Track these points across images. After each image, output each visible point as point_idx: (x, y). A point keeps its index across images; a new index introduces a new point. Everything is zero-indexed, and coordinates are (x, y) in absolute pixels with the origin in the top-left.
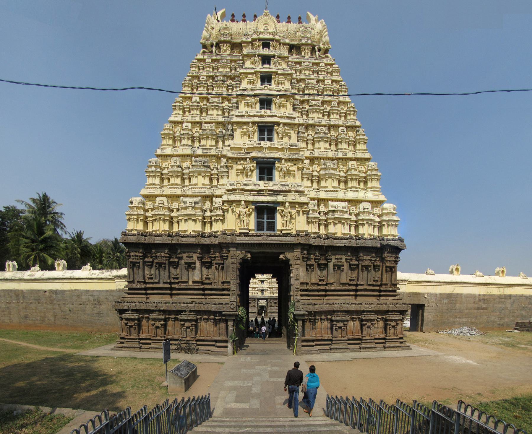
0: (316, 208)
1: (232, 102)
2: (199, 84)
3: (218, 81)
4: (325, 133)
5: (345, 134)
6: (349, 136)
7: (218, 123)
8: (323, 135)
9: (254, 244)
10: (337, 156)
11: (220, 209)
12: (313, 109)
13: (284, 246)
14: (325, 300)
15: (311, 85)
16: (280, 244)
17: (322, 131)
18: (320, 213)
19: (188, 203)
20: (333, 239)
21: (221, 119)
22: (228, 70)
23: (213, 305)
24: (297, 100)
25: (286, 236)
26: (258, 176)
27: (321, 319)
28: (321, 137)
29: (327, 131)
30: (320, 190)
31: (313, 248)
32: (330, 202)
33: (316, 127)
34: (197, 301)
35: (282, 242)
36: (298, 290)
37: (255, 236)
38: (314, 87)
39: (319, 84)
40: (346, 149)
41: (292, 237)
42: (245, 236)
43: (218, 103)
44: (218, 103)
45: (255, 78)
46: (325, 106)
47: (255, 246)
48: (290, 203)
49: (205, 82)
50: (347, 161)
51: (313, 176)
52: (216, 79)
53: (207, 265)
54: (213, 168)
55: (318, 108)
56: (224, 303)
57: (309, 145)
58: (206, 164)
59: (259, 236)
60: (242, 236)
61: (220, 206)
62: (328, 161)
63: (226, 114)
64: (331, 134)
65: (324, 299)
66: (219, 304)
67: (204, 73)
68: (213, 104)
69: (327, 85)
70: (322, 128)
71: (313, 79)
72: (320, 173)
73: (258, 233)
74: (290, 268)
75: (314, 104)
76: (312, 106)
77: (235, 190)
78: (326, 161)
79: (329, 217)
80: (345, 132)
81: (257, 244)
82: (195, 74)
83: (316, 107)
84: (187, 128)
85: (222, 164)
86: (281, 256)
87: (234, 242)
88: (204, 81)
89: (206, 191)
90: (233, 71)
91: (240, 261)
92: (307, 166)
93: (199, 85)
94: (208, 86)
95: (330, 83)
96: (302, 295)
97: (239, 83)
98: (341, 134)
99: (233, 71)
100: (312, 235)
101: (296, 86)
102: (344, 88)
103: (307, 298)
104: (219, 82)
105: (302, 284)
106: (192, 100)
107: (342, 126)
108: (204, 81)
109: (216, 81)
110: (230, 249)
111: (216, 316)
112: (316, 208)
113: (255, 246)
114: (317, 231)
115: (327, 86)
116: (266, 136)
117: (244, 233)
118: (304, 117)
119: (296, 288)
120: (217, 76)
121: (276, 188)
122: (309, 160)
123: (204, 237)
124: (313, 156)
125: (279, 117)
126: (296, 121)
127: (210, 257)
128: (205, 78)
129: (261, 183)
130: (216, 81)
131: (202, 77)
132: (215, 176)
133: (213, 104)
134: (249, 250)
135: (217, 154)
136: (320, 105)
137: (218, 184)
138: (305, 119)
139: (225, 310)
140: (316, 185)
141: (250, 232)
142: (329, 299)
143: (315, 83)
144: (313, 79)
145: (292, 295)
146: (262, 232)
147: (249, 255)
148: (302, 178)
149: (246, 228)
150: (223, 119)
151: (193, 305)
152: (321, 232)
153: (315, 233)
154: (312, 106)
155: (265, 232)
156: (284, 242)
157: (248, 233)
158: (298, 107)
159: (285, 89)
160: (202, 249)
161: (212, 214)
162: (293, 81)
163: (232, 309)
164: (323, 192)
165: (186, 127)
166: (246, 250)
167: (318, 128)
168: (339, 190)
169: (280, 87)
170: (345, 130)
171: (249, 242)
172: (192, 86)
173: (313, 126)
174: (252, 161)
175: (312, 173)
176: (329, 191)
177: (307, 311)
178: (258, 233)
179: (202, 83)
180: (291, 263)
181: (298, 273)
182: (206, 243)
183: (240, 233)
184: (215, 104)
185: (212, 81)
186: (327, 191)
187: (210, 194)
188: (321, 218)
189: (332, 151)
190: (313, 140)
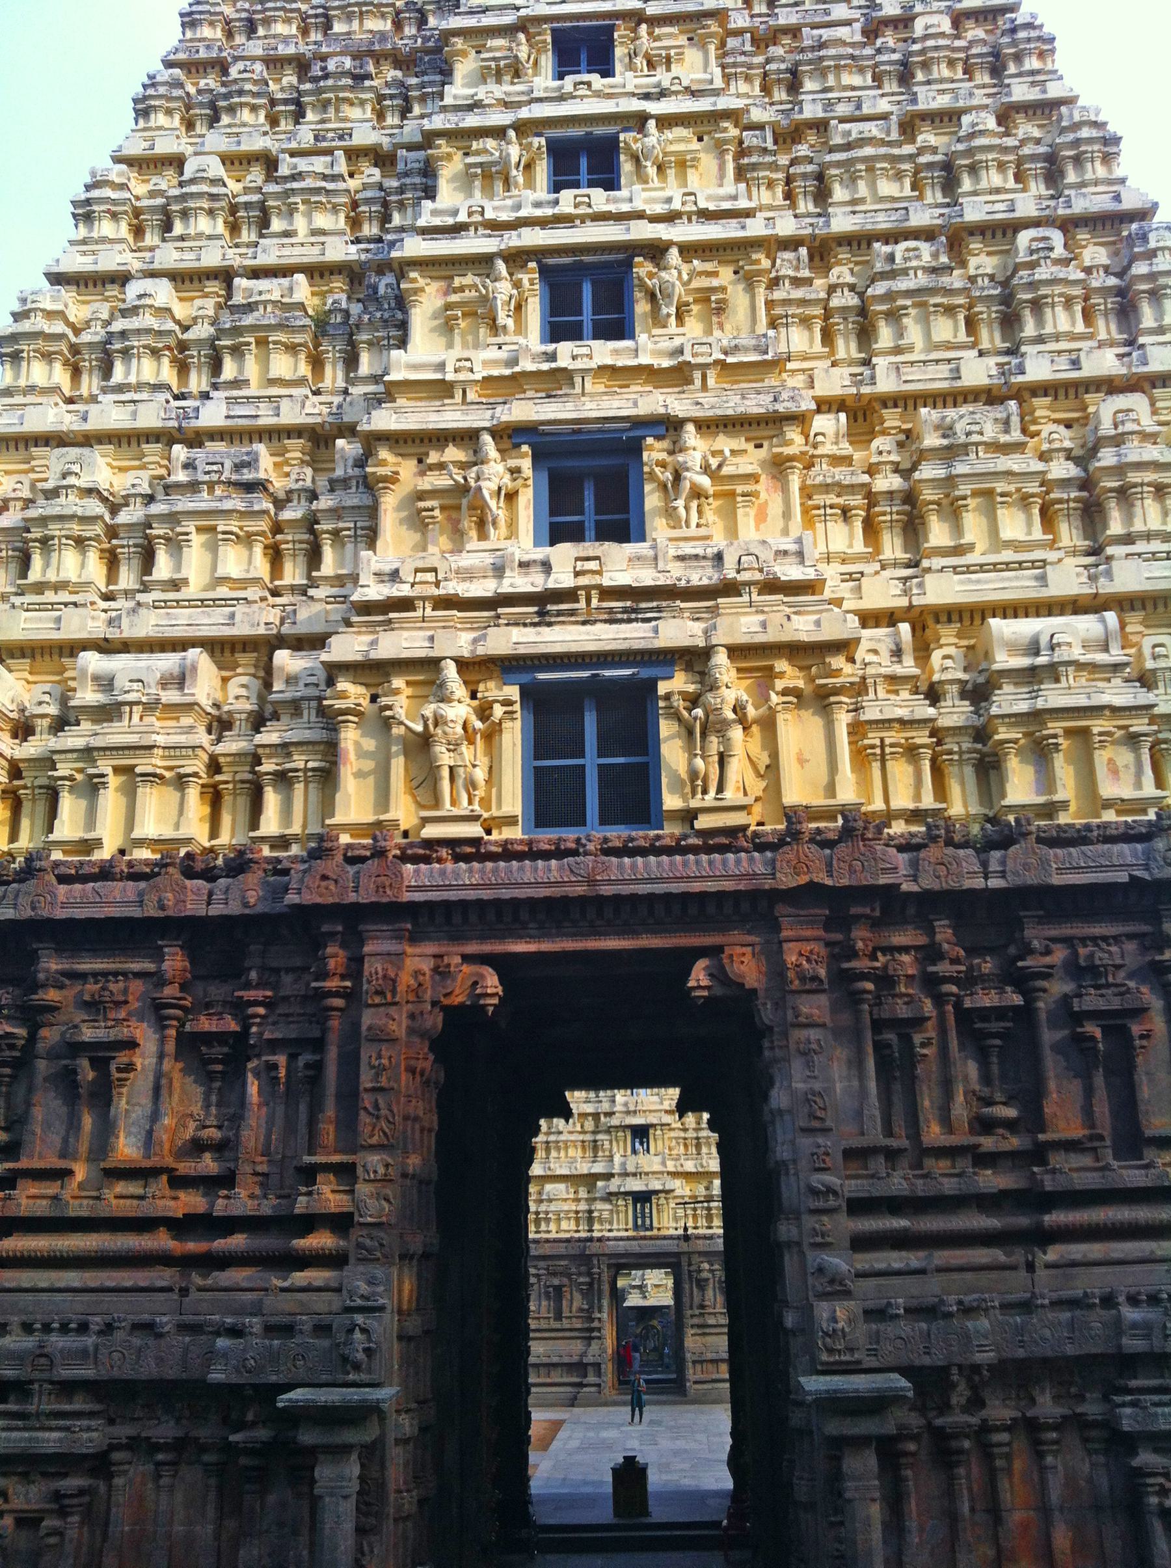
0: (908, 666)
1: (400, 166)
2: (227, 96)
3: (326, 77)
4: (934, 270)
5: (1057, 262)
6: (1088, 270)
7: (317, 272)
8: (922, 280)
9: (515, 903)
10: (1020, 379)
11: (309, 714)
12: (851, 162)
13: (711, 909)
14: (1041, 1273)
15: (832, 52)
16: (686, 897)
17: (914, 263)
18: (934, 695)
19: (121, 682)
20: (1039, 840)
21: (340, 250)
22: (388, 26)
23: (222, 1342)
24: (760, 127)
25: (722, 849)
26: (546, 520)
27: (1031, 1427)
28: (908, 293)
29: (944, 259)
30: (928, 570)
31: (911, 911)
32: (995, 623)
33: (877, 245)
34: (125, 1309)
35: (696, 887)
36: (832, 1202)
37: (520, 856)
38: (853, 57)
39: (879, 42)
40: (1074, 337)
41: (761, 847)
42: (457, 858)
43: (325, 177)
44: (325, 177)
45: (523, 52)
46: (920, 138)
47: (524, 915)
48: (735, 651)
49: (255, 89)
50: (1088, 397)
51: (871, 498)
52: (316, 71)
53: (219, 1051)
54: (290, 492)
55: (883, 150)
56: (306, 1322)
57: (840, 343)
58: (247, 476)
59: (546, 855)
60: (440, 860)
61: (314, 692)
62: (963, 410)
63: (370, 229)
64: (972, 272)
65: (1030, 1267)
66: (270, 1330)
67: (255, 48)
68: (295, 185)
69: (926, 37)
70: (911, 244)
71: (848, 23)
72: (917, 475)
73: (546, 837)
74: (760, 1049)
75: (854, 135)
76: (848, 147)
77: (405, 604)
78: (951, 413)
79: (994, 710)
80: (1059, 251)
81: (532, 904)
82: (203, 54)
83: (868, 151)
84: (148, 301)
85: (339, 473)
86: (699, 976)
87: (388, 897)
88: (255, 82)
89: (238, 618)
90: (410, 30)
91: (435, 1021)
92: (828, 449)
93: (222, 103)
94: (273, 102)
95: (946, 25)
96: (861, 1243)
97: (438, 78)
98: (1033, 265)
99: (410, 30)
100: (898, 828)
101: (750, 67)
102: (1029, 40)
103: (895, 1259)
104: (330, 82)
105: (856, 1155)
106: (182, 174)
107: (1036, 223)
108: (255, 82)
109: (315, 80)
110: (367, 949)
111: (241, 1426)
112: (908, 666)
113: (524, 915)
114: (928, 801)
115: (930, 43)
116: (587, 316)
117: (451, 843)
118: (806, 205)
119: (814, 1192)
120: (324, 58)
121: (646, 577)
122: (843, 416)
123: (209, 875)
124: (866, 390)
125: (655, 219)
126: (756, 228)
127: (239, 1008)
128: (258, 67)
129: (564, 554)
130: (315, 80)
131: (240, 65)
132: (298, 537)
133: (295, 185)
134: (487, 948)
135: (310, 420)
136: (895, 135)
137: (309, 577)
138: (809, 215)
139: (302, 1374)
140: (898, 542)
141: (495, 836)
142: (1074, 1264)
143: (858, 38)
144: (848, 23)
145: (789, 1244)
146: (569, 835)
147: (492, 982)
148: (805, 511)
149: (463, 808)
150: (353, 249)
151: (90, 1341)
152: (956, 809)
153: (915, 816)
154: (848, 147)
155: (596, 832)
156: (711, 886)
157: (476, 842)
158: (769, 159)
159: (685, 83)
160: (193, 952)
161: (260, 739)
162: (732, 43)
163: (357, 1367)
164: (949, 575)
165: (140, 297)
166: (472, 948)
167: (887, 249)
168: (1052, 556)
169: (662, 77)
170: (1057, 238)
171: (486, 895)
172: (188, 108)
173: (859, 241)
174: (507, 444)
175: (866, 478)
176: (982, 568)
177: (904, 1371)
178: (546, 837)
179: (241, 93)
180: (767, 1013)
181: (817, 1086)
182: (216, 910)
183: (430, 844)
184: (309, 183)
185: (294, 80)
186: (968, 569)
187: (262, 630)
188: (945, 722)
189: (981, 354)
190: (863, 311)
